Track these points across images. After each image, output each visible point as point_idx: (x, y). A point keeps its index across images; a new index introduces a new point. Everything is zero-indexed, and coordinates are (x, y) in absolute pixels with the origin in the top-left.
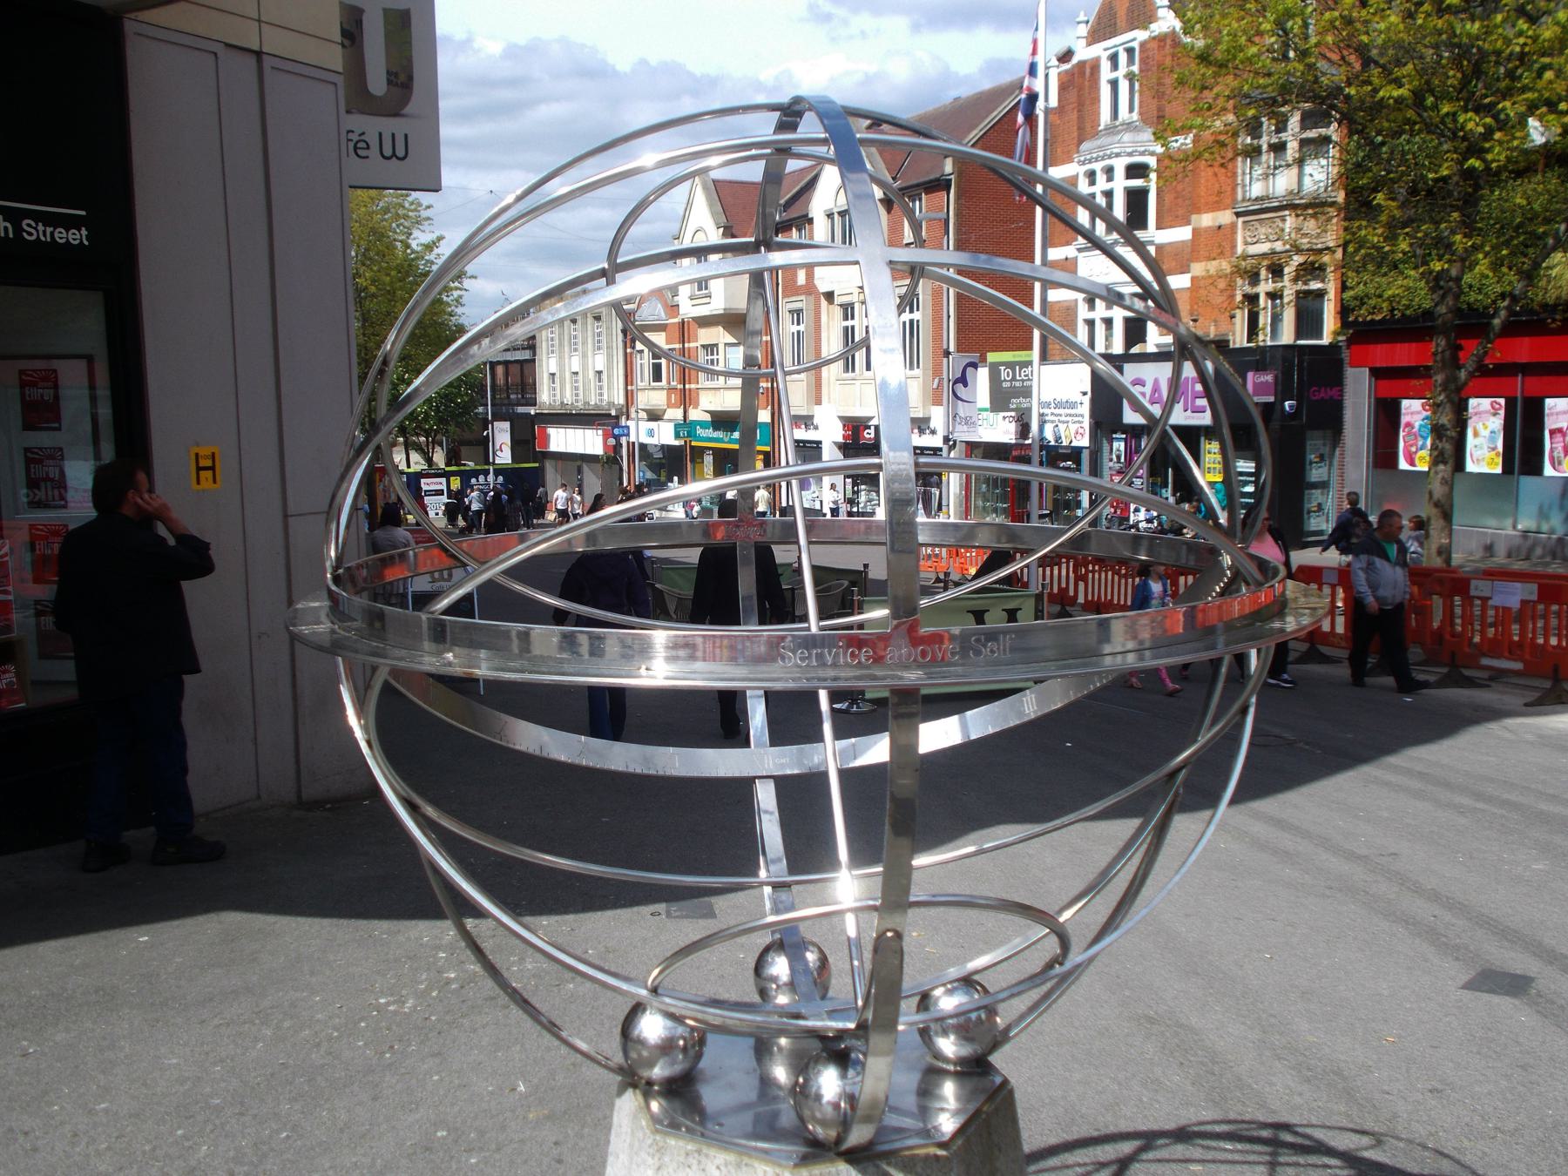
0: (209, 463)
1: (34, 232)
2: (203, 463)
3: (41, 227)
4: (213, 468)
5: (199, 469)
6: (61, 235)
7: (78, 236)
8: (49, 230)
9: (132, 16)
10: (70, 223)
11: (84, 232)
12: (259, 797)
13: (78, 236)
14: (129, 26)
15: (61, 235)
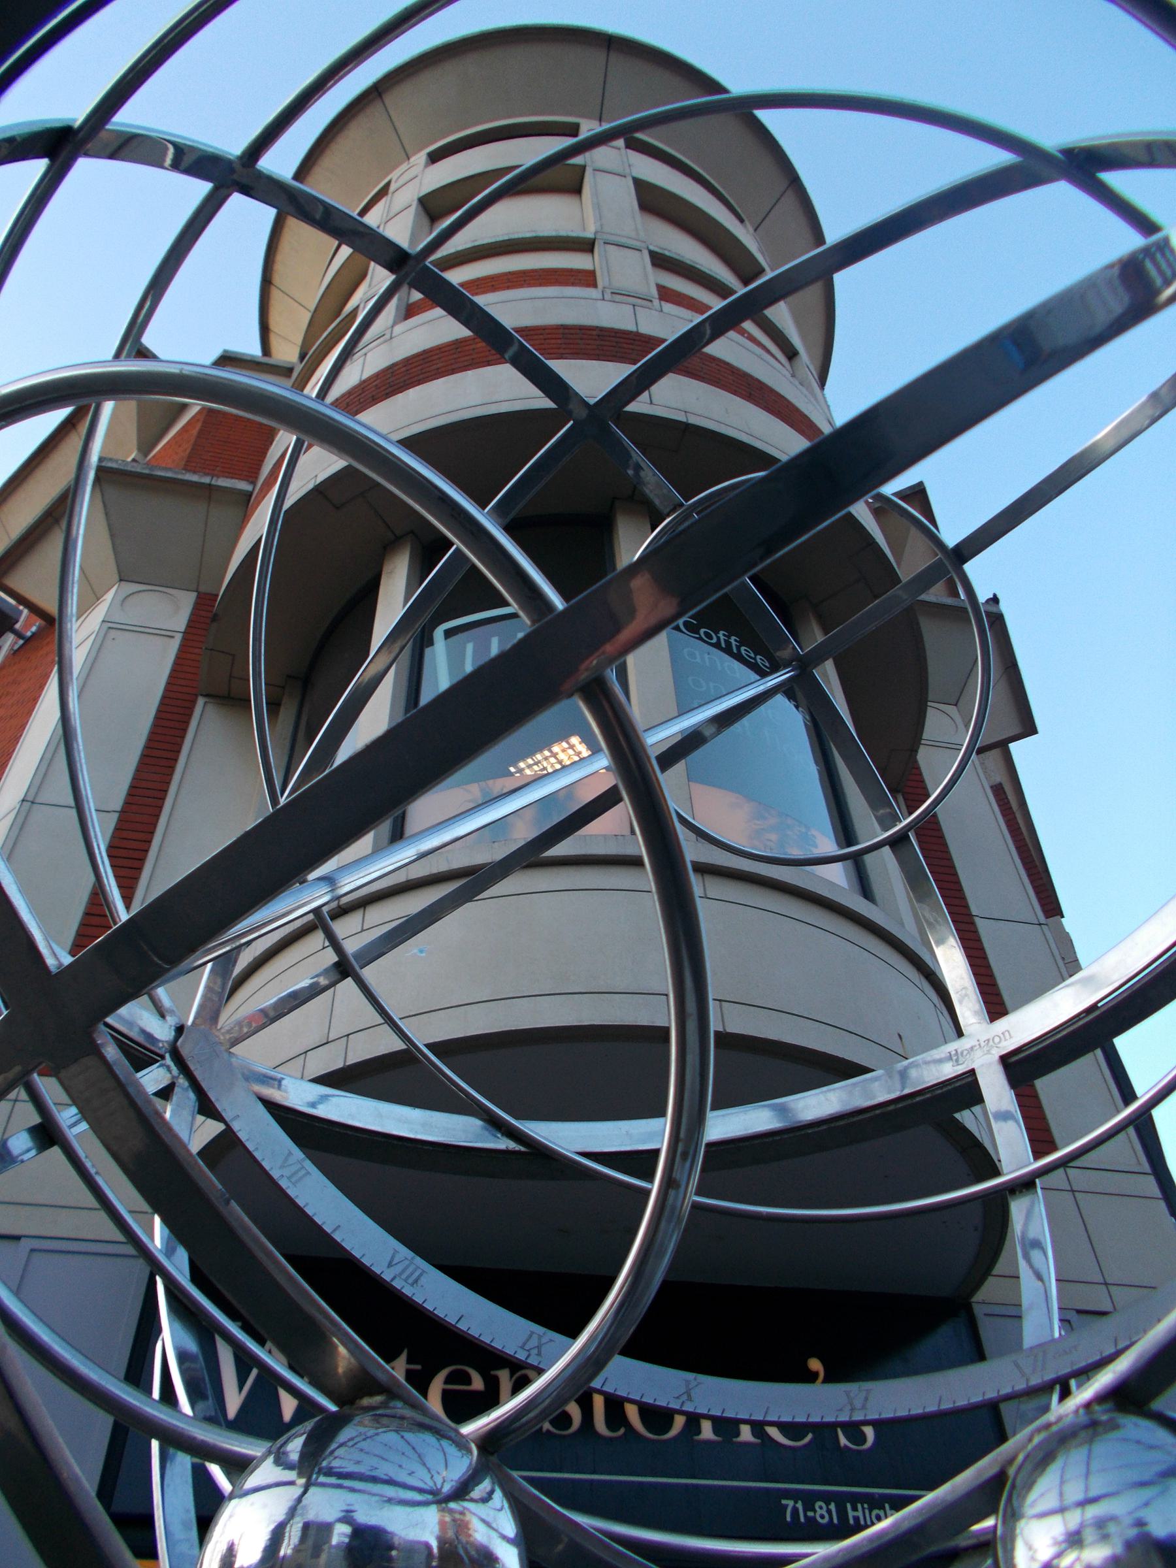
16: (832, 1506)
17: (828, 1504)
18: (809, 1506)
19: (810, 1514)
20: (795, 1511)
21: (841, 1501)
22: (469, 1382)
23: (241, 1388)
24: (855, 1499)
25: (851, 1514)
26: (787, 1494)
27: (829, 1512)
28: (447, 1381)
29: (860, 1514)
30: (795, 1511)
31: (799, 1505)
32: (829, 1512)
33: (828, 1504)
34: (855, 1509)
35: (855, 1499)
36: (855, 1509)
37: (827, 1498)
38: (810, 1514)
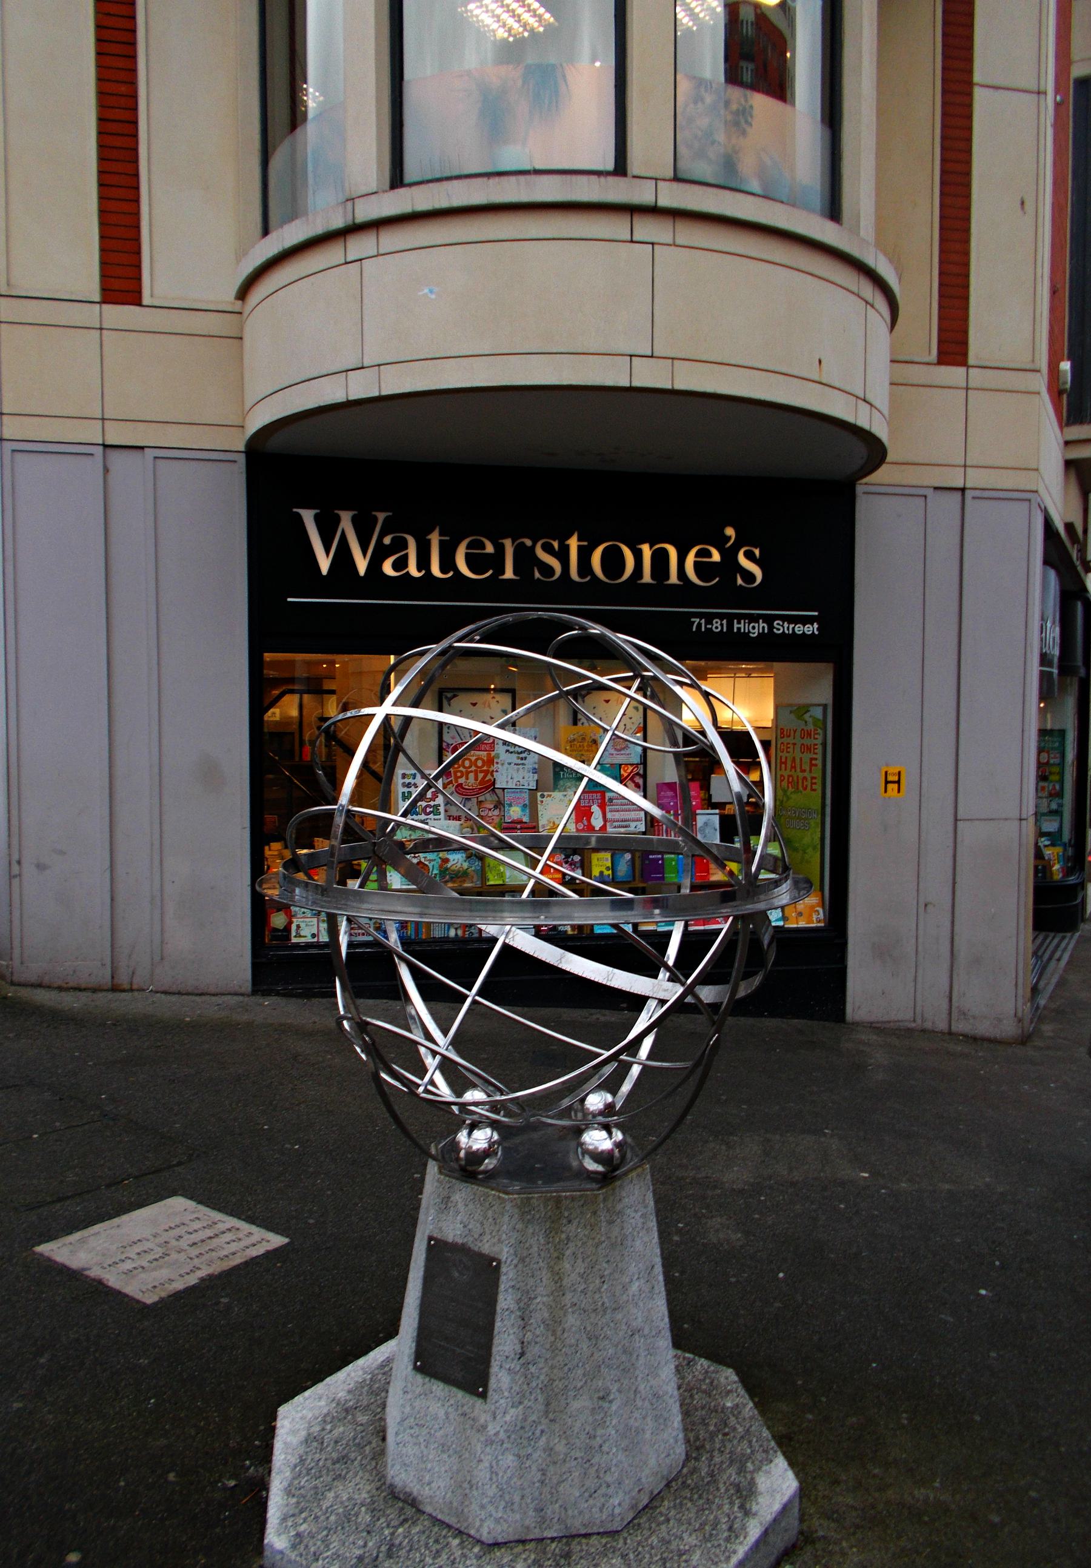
0: (896, 779)
1: (782, 628)
2: (890, 778)
3: (786, 625)
4: (898, 782)
5: (887, 782)
6: (799, 629)
7: (811, 629)
8: (791, 626)
9: (864, 480)
10: (804, 620)
11: (816, 625)
12: (914, 1021)
13: (811, 629)
14: (860, 489)
15: (799, 629)
16: (725, 622)
17: (722, 620)
18: (709, 621)
19: (709, 626)
20: (699, 624)
21: (730, 618)
22: (484, 548)
23: (328, 555)
24: (740, 617)
25: (736, 626)
26: (696, 615)
27: (722, 625)
28: (468, 548)
29: (742, 626)
30: (699, 624)
31: (703, 621)
32: (722, 625)
33: (722, 620)
34: (739, 623)
35: (740, 617)
36: (739, 623)
37: (721, 616)
38: (709, 626)
